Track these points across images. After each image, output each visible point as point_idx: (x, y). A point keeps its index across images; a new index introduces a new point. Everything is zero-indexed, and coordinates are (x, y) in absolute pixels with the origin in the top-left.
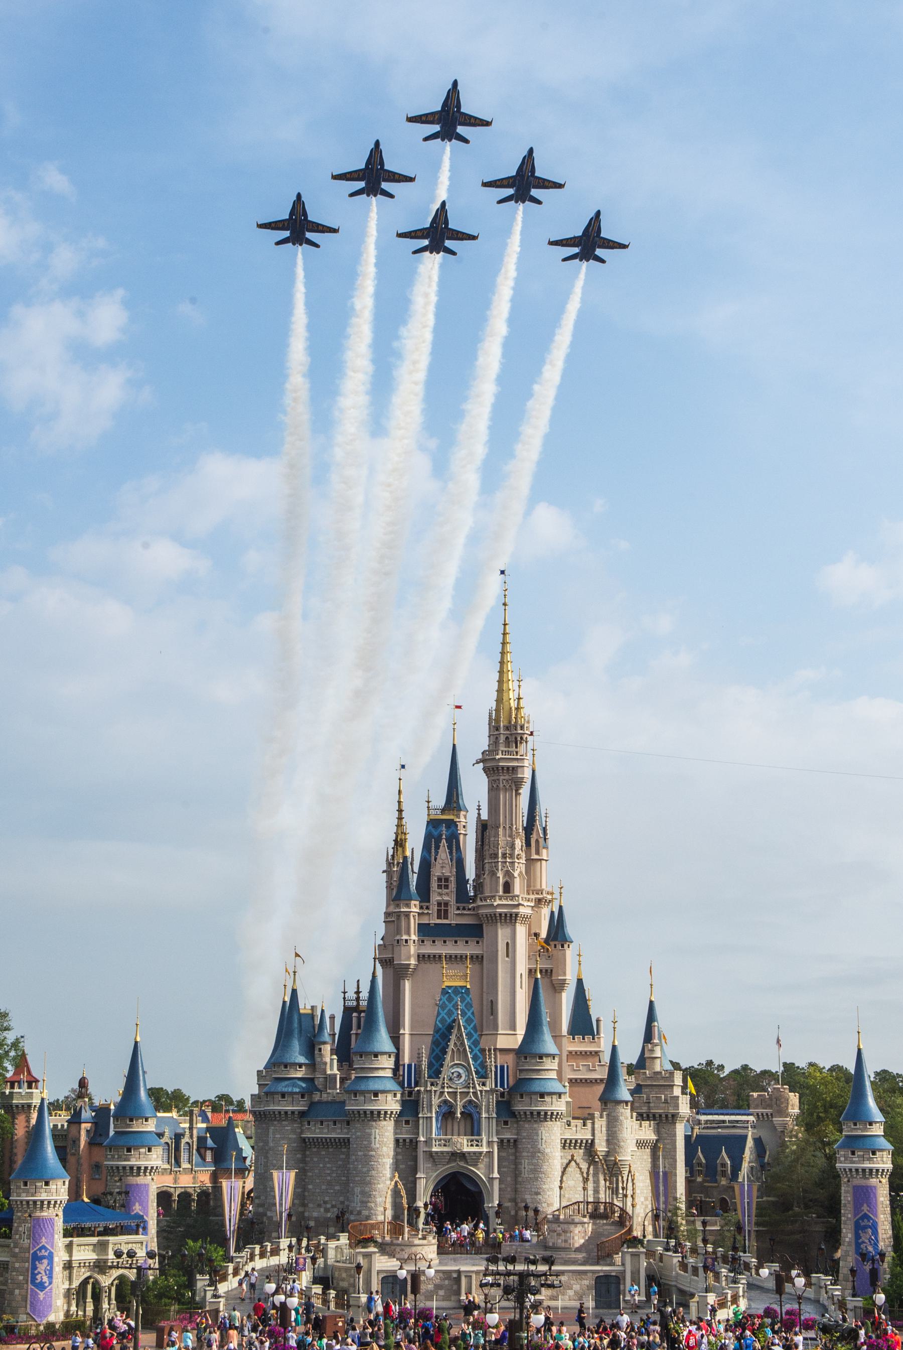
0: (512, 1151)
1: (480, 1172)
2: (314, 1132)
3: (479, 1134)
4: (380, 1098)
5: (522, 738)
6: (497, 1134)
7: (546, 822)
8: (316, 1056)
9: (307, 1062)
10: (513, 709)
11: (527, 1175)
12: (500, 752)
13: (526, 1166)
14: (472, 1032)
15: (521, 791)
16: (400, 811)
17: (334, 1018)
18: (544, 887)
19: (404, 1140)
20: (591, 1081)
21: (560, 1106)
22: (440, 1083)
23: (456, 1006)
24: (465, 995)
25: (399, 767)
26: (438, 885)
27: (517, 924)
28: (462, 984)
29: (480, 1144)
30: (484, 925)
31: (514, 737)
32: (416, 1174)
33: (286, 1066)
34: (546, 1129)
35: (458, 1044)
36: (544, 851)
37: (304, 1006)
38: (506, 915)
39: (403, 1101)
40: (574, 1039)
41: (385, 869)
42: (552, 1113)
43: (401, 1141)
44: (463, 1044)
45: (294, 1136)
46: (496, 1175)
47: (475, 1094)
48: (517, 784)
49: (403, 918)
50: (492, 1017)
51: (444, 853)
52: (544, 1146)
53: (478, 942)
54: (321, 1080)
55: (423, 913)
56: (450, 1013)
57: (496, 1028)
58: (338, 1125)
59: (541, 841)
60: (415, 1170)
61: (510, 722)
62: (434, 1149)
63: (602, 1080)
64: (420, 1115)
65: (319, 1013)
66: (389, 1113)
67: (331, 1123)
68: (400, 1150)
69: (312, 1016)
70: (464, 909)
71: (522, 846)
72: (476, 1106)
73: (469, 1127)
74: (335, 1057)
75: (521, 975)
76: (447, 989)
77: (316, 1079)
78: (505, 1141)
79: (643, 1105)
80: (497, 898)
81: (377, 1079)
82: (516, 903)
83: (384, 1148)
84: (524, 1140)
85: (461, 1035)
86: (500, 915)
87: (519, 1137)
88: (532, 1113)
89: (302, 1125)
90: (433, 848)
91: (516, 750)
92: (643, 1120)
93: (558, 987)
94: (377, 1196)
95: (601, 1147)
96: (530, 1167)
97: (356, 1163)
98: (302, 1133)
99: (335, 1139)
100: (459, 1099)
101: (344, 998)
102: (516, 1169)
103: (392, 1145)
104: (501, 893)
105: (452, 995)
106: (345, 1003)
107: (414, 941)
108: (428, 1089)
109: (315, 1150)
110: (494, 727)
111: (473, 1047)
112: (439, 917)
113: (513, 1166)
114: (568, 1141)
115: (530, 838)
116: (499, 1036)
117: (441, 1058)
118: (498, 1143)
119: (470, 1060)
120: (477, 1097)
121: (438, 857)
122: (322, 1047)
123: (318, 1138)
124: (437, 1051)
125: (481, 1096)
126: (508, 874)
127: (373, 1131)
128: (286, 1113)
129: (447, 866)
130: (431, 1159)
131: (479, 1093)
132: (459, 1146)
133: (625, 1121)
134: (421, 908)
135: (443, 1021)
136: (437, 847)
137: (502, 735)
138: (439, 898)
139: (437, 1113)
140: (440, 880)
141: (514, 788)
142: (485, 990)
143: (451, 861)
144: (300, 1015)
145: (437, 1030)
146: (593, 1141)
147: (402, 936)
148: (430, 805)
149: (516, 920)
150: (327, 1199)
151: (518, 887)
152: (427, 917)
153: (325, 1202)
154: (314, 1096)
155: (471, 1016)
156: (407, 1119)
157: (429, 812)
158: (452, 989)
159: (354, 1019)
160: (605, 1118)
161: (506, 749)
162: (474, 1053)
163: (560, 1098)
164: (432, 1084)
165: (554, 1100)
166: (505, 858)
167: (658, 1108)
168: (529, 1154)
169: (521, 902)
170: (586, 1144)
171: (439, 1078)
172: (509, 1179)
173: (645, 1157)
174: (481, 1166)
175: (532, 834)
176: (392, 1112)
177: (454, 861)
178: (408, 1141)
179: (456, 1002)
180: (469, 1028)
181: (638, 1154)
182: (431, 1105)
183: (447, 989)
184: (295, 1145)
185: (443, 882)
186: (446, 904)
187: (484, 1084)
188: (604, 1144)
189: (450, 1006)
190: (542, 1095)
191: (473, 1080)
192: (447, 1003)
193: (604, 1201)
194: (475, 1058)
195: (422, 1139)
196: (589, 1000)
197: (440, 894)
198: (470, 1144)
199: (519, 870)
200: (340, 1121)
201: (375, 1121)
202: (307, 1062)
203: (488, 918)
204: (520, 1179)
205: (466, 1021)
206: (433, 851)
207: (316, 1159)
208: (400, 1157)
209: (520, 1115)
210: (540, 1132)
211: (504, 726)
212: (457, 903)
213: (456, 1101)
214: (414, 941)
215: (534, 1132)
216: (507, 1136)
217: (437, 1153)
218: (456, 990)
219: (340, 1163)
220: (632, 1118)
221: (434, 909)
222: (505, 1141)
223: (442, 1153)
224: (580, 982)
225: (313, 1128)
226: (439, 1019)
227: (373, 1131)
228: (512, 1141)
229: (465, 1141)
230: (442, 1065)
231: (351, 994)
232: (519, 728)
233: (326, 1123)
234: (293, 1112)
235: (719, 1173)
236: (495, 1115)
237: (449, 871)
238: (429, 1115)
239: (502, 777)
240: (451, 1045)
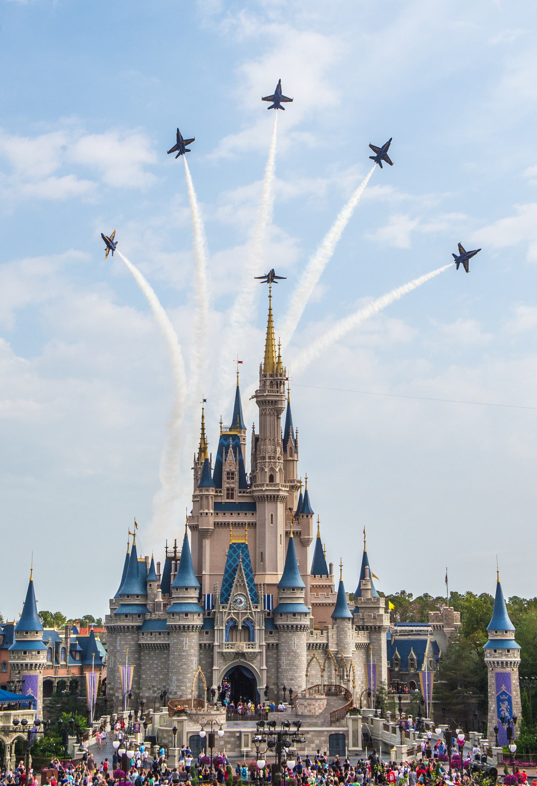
1: (255, 666)
2: (146, 640)
3: (253, 640)
4: (189, 617)
5: (281, 382)
6: (265, 640)
7: (297, 436)
8: (148, 589)
10: (275, 363)
11: (285, 667)
12: (267, 391)
15: (280, 416)
16: (203, 429)
17: (160, 564)
18: (295, 478)
19: (205, 645)
20: (326, 605)
21: (306, 621)
22: (228, 606)
23: (238, 556)
24: (244, 549)
25: (202, 401)
26: (227, 477)
27: (278, 502)
28: (243, 541)
29: (254, 647)
30: (257, 503)
31: (276, 381)
32: (213, 667)
33: (128, 597)
34: (297, 636)
35: (240, 581)
36: (296, 455)
37: (141, 556)
38: (271, 496)
39: (204, 619)
40: (315, 577)
41: (193, 467)
42: (301, 626)
43: (203, 645)
44: (243, 581)
45: (133, 643)
46: (265, 667)
47: (251, 613)
48: (279, 412)
49: (204, 498)
50: (262, 563)
51: (231, 457)
52: (296, 648)
53: (253, 514)
54: (151, 605)
55: (217, 496)
56: (235, 561)
57: (264, 569)
58: (162, 635)
59: (293, 448)
60: (212, 665)
61: (273, 372)
62: (225, 650)
63: (333, 604)
64: (216, 628)
65: (150, 561)
67: (157, 634)
68: (202, 651)
69: (145, 563)
70: (244, 492)
71: (281, 451)
72: (252, 622)
73: (247, 635)
74: (160, 590)
75: (281, 535)
76: (233, 545)
77: (147, 605)
78: (271, 645)
79: (360, 620)
80: (265, 485)
81: (187, 604)
82: (277, 488)
84: (283, 644)
85: (242, 575)
86: (267, 496)
87: (280, 642)
88: (288, 626)
89: (139, 635)
90: (224, 453)
91: (277, 390)
92: (360, 630)
93: (305, 543)
94: (187, 682)
95: (332, 648)
97: (173, 660)
98: (138, 640)
99: (160, 644)
100: (240, 617)
101: (167, 551)
102: (278, 663)
103: (197, 648)
104: (268, 482)
105: (236, 549)
106: (167, 555)
107: (212, 515)
108: (221, 610)
109: (146, 652)
110: (263, 375)
111: (250, 583)
112: (228, 498)
113: (275, 662)
114: (311, 645)
115: (286, 446)
117: (229, 590)
118: (266, 646)
119: (248, 591)
120: (252, 616)
121: (227, 459)
122: (152, 583)
123: (148, 644)
124: (226, 585)
126: (272, 469)
127: (185, 639)
128: (128, 627)
129: (233, 465)
130: (223, 658)
131: (253, 613)
132: (240, 648)
133: (348, 631)
134: (216, 492)
135: (230, 566)
136: (227, 453)
137: (268, 380)
138: (228, 486)
139: (226, 626)
140: (228, 473)
141: (276, 414)
142: (257, 545)
143: (236, 461)
144: (138, 562)
145: (226, 571)
146: (327, 644)
147: (204, 510)
148: (222, 426)
149: (277, 499)
150: (154, 684)
151: (278, 479)
152: (220, 498)
153: (153, 687)
154: (146, 616)
155: (249, 563)
156: (207, 630)
157: (221, 430)
158: (236, 545)
159: (172, 565)
160: (335, 629)
161: (271, 389)
162: (250, 587)
163: (306, 616)
164: (223, 608)
165: (302, 617)
166: (270, 459)
167: (370, 622)
169: (281, 488)
170: (323, 646)
171: (228, 603)
172: (273, 670)
173: (361, 655)
175: (287, 444)
176: (197, 626)
177: (238, 462)
178: (207, 645)
179: (239, 554)
180: (247, 570)
181: (357, 652)
182: (222, 622)
183: (233, 545)
184: (134, 648)
185: (231, 475)
186: (232, 489)
188: (335, 646)
189: (235, 556)
190: (294, 614)
191: (249, 604)
192: (233, 554)
193: (335, 684)
194: (251, 590)
196: (325, 552)
197: (228, 483)
198: (247, 647)
199: (279, 467)
200: (164, 633)
201: (186, 632)
202: (142, 593)
203: (259, 498)
204: (280, 670)
206: (224, 455)
207: (147, 658)
208: (202, 656)
209: (280, 628)
210: (293, 639)
211: (269, 374)
212: (239, 488)
214: (212, 513)
215: (289, 638)
216: (272, 641)
217: (226, 653)
218: (239, 545)
219: (163, 660)
220: (352, 629)
221: (224, 493)
222: (271, 645)
223: (230, 653)
224: (319, 540)
225: (146, 637)
226: (228, 564)
227: (185, 639)
228: (275, 645)
229: (245, 646)
230: (229, 595)
231: (171, 549)
232: (279, 375)
234: (133, 627)
235: (409, 665)
236: (264, 628)
237: (234, 468)
238: (221, 628)
239: (268, 407)
240: (235, 581)
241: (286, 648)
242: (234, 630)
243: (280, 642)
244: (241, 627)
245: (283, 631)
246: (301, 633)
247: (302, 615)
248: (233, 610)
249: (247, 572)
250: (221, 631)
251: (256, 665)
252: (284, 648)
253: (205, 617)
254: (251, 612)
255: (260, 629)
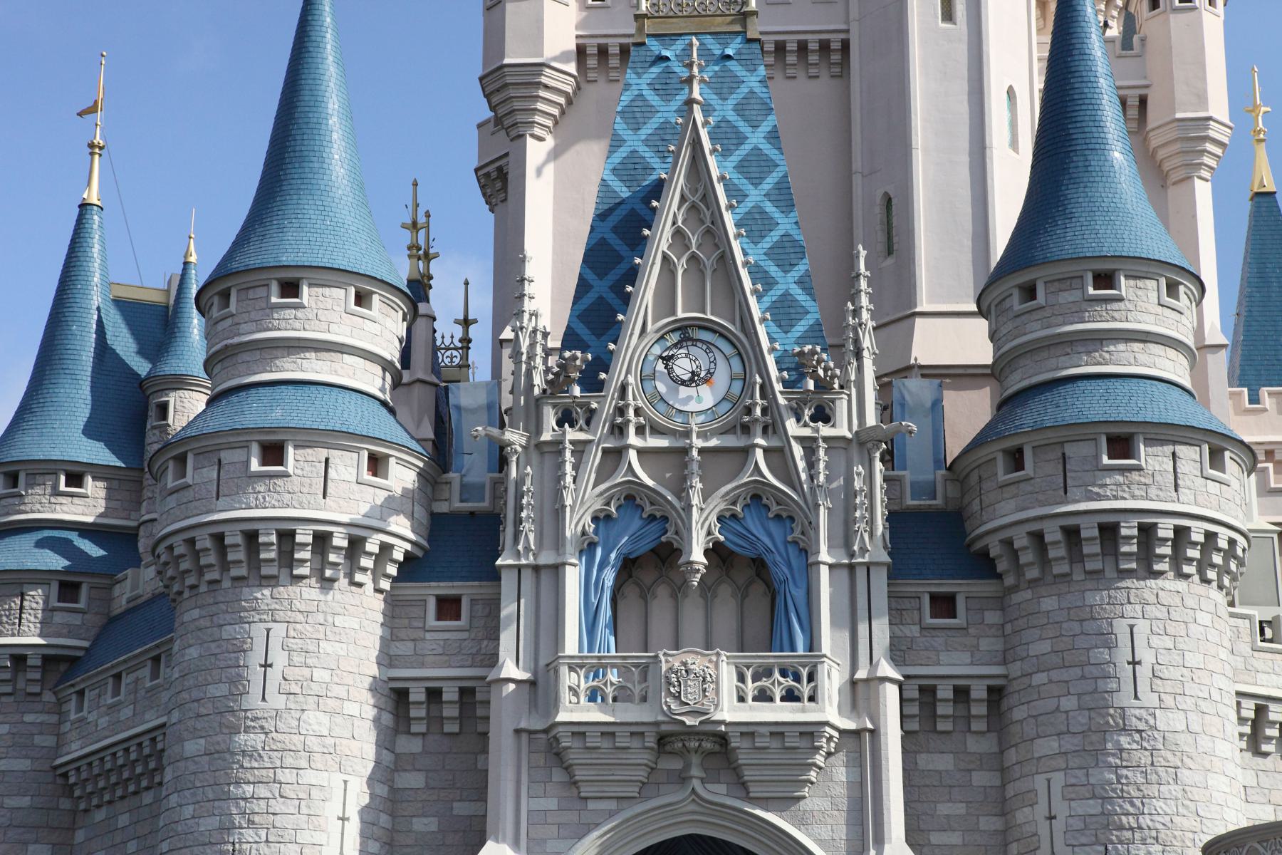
0: (980, 745)
9: (113, 461)
13: (1060, 808)
14: (769, 208)
19: (434, 695)
29: (805, 689)
34: (1152, 611)
40: (1254, 399)
43: (417, 695)
45: (24, 764)
47: (779, 457)
50: (890, 261)
52: (1148, 699)
66: (340, 541)
68: (415, 746)
75: (1011, 92)
83: (310, 716)
84: (1040, 678)
85: (708, 197)
88: (1072, 534)
96: (1080, 808)
98: (57, 749)
108: (546, 436)
111: (773, 269)
113: (989, 823)
116: (919, 321)
124: (601, 287)
125: (811, 465)
130: (558, 775)
131: (798, 451)
132: (691, 692)
142: (857, 164)
155: (767, 148)
156: (446, 588)
164: (566, 418)
165: (1183, 467)
168: (1070, 743)
171: (598, 386)
174: (813, 802)
178: (450, 694)
180: (755, 196)
184: (25, 801)
187: (822, 415)
191: (766, 390)
195: (510, 669)
198: (750, 688)
201: (272, 581)
202: (113, 461)
205: (741, 167)
208: (413, 780)
209: (1014, 554)
210: (1121, 627)
213: (681, 490)
217: (580, 730)
222: (945, 692)
225: (91, 718)
227: (258, 631)
233: (131, 677)
240: (662, 239)
241: (1069, 703)
242: (662, 591)
243: (1015, 669)
244: (707, 553)
245: (1033, 583)
246: (1181, 585)
247: (1181, 449)
248: (640, 430)
249: (749, 204)
250: (545, 577)
251: (825, 833)
252: (1050, 704)
253: (442, 508)
254: (775, 443)
255: (851, 568)
